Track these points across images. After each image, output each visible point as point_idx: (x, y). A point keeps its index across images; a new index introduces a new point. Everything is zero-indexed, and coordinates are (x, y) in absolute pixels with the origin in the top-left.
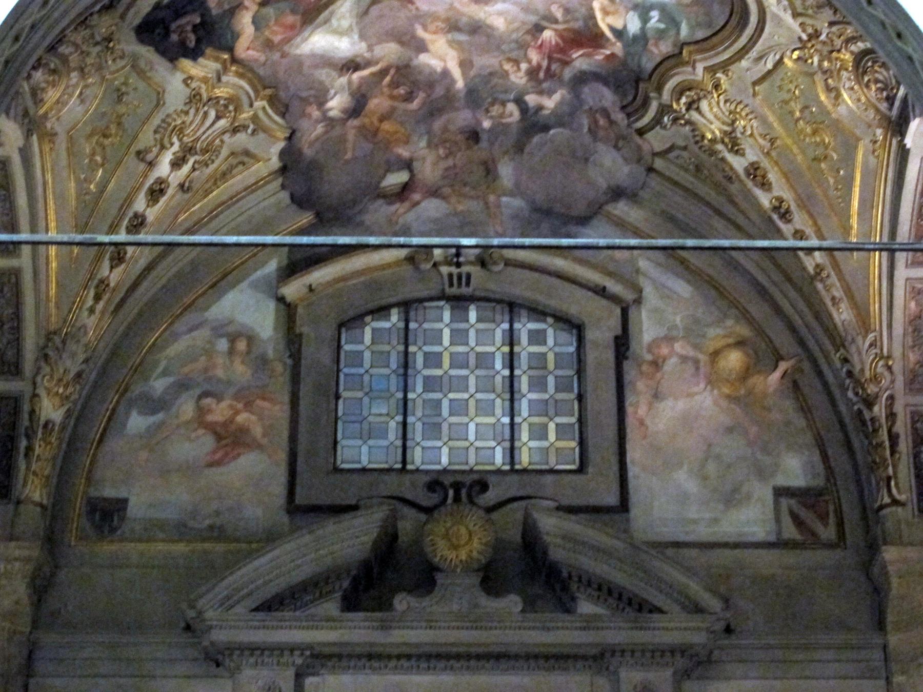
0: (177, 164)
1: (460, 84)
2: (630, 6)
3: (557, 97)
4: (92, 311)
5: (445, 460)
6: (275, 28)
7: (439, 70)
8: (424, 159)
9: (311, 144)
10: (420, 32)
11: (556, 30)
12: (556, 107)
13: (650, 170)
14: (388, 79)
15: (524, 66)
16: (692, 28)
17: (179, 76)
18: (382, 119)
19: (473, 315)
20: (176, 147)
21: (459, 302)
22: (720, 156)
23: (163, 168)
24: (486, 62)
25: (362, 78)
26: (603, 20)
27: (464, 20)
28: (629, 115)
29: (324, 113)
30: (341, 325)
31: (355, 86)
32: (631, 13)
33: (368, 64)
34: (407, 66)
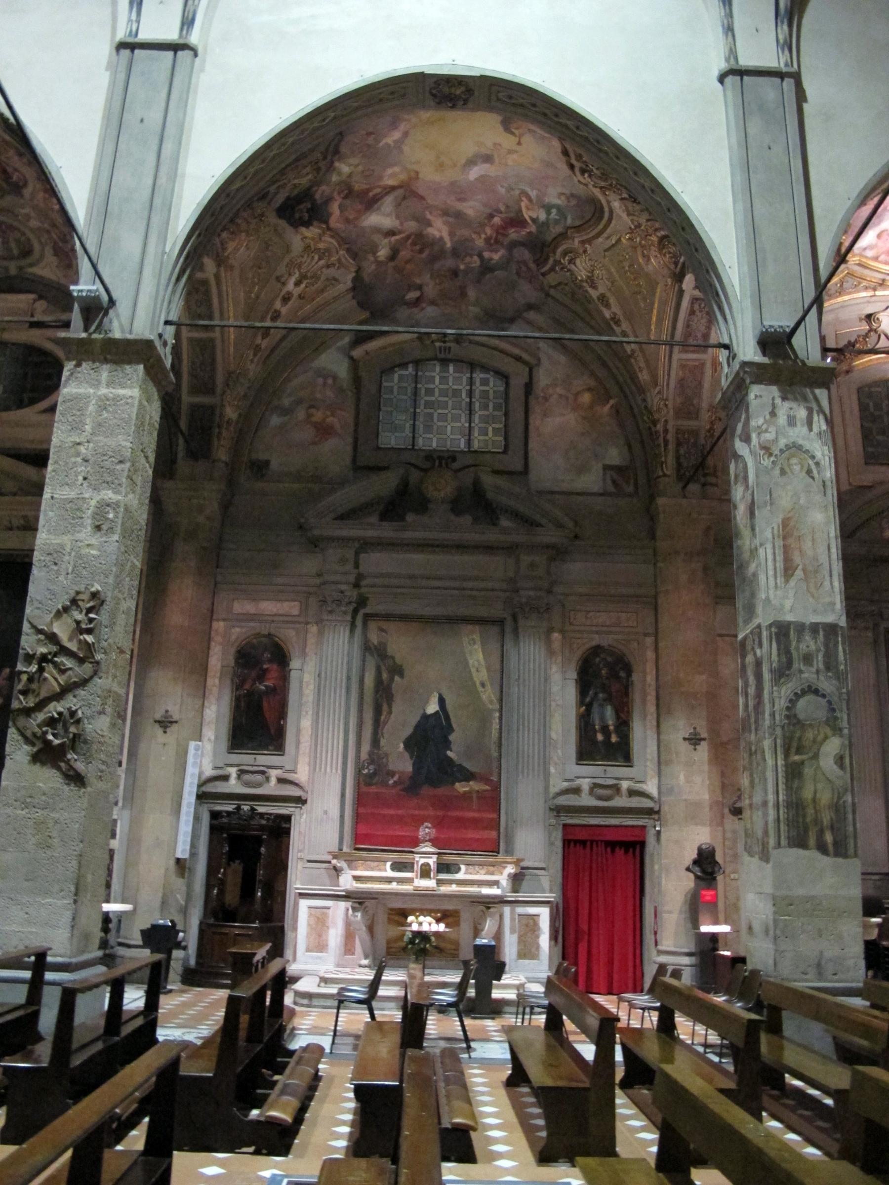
0: (297, 284)
1: (449, 245)
4: (252, 361)
5: (434, 445)
7: (438, 236)
10: (428, 216)
12: (500, 258)
13: (548, 295)
14: (410, 241)
15: (483, 236)
16: (573, 219)
17: (299, 237)
19: (451, 369)
20: (297, 275)
21: (445, 362)
23: (290, 286)
24: (465, 232)
25: (397, 240)
28: (538, 265)
29: (376, 258)
30: (383, 372)
33: (400, 232)
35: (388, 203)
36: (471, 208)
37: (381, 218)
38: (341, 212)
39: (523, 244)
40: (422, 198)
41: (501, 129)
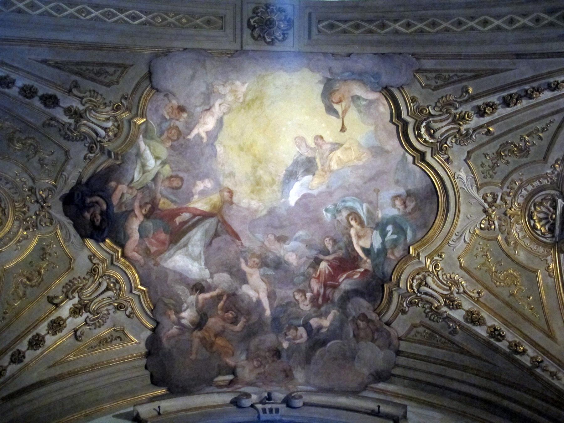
0: (75, 312)
1: (268, 313)
2: (374, 226)
3: (330, 317)
6: (153, 240)
7: (254, 299)
8: (244, 367)
9: (169, 338)
10: (244, 267)
11: (328, 261)
13: (398, 353)
14: (221, 304)
15: (309, 295)
16: (414, 232)
17: (85, 254)
18: (216, 336)
20: (76, 300)
22: (445, 315)
24: (286, 293)
25: (205, 299)
26: (358, 244)
27: (271, 256)
28: (379, 314)
29: (180, 319)
31: (200, 305)
32: (375, 232)
33: (209, 288)
34: (234, 294)
35: (197, 237)
36: (292, 253)
37: (186, 261)
38: (141, 237)
39: (356, 292)
40: (236, 236)
41: (321, 106)
